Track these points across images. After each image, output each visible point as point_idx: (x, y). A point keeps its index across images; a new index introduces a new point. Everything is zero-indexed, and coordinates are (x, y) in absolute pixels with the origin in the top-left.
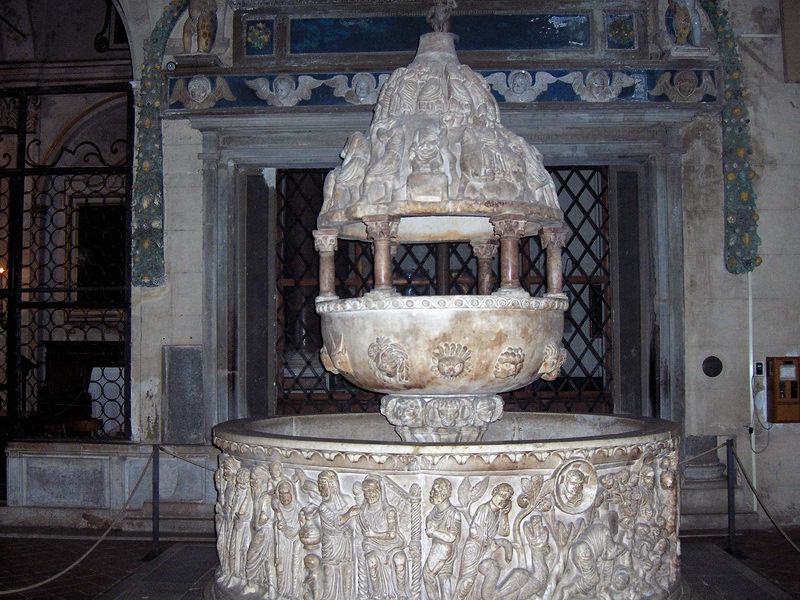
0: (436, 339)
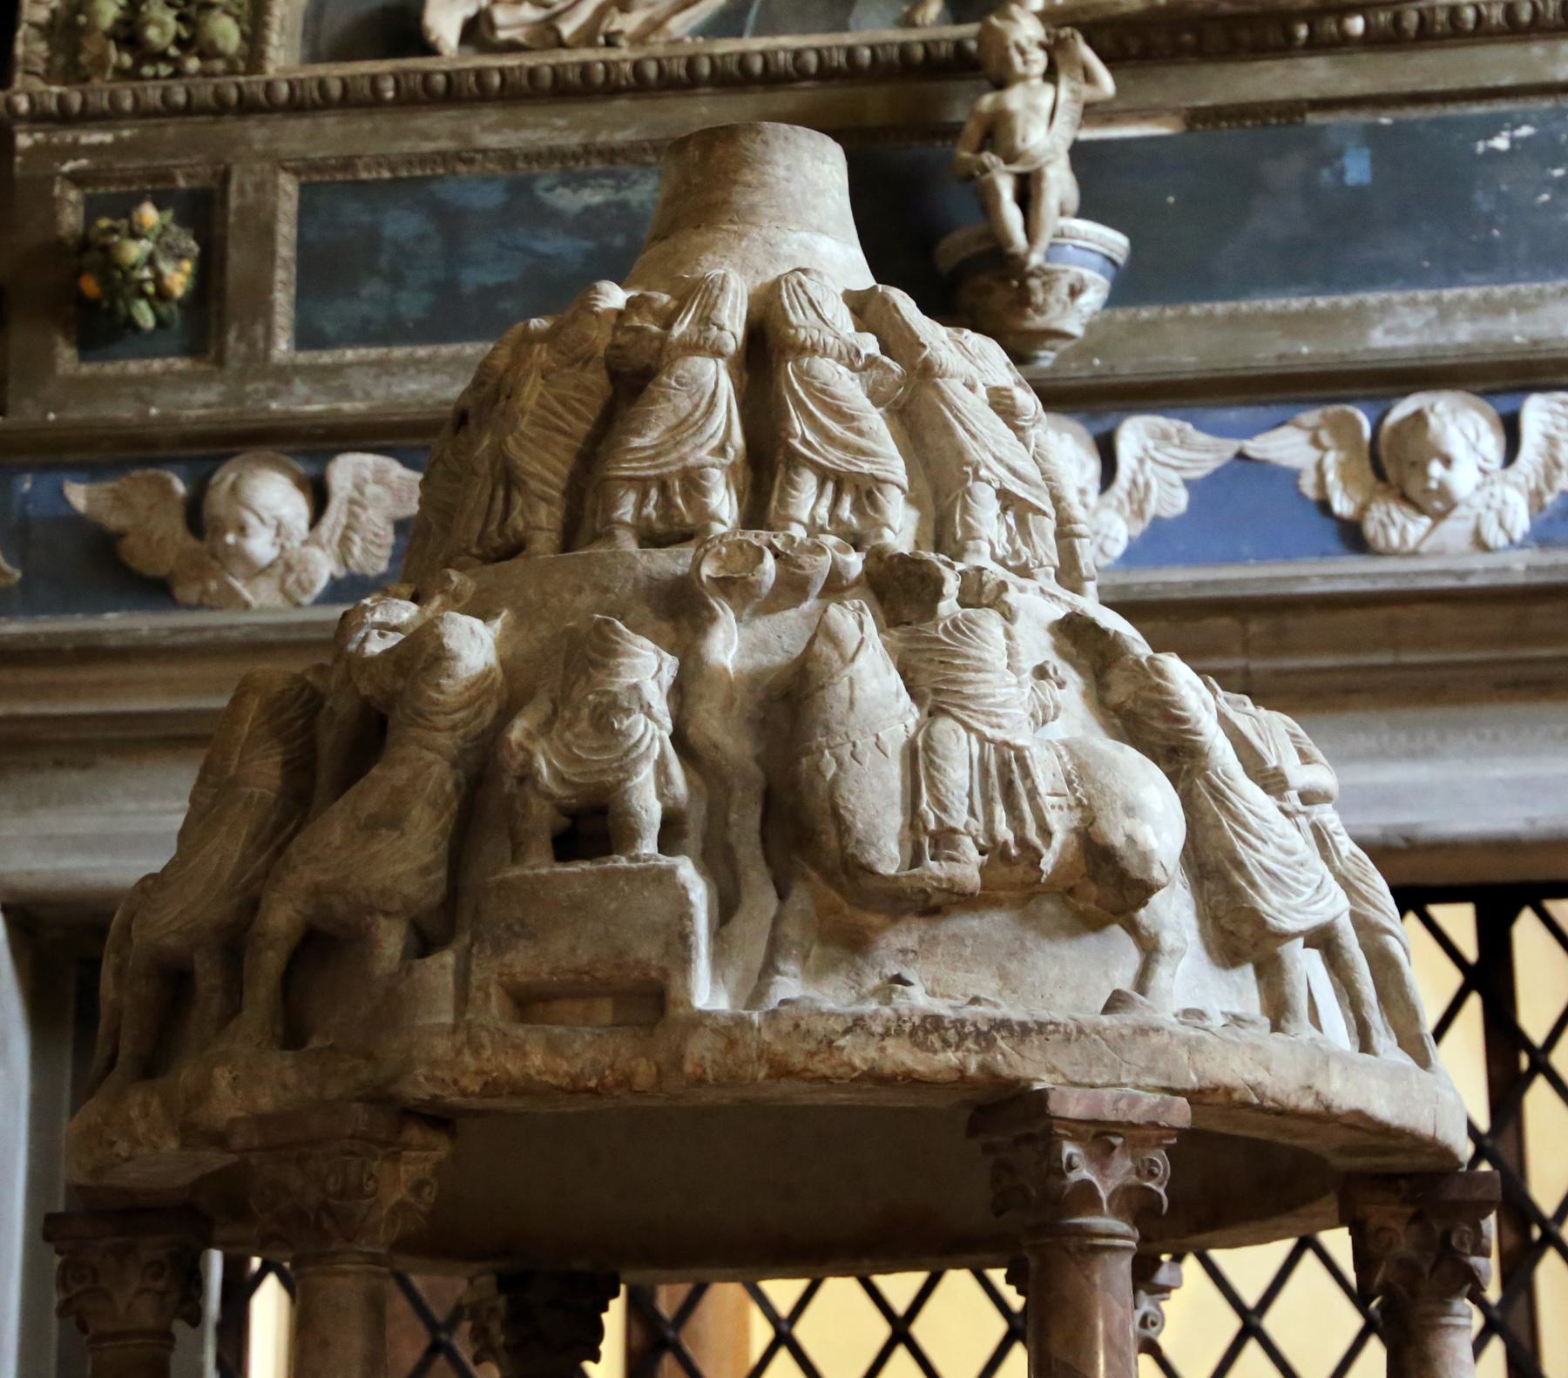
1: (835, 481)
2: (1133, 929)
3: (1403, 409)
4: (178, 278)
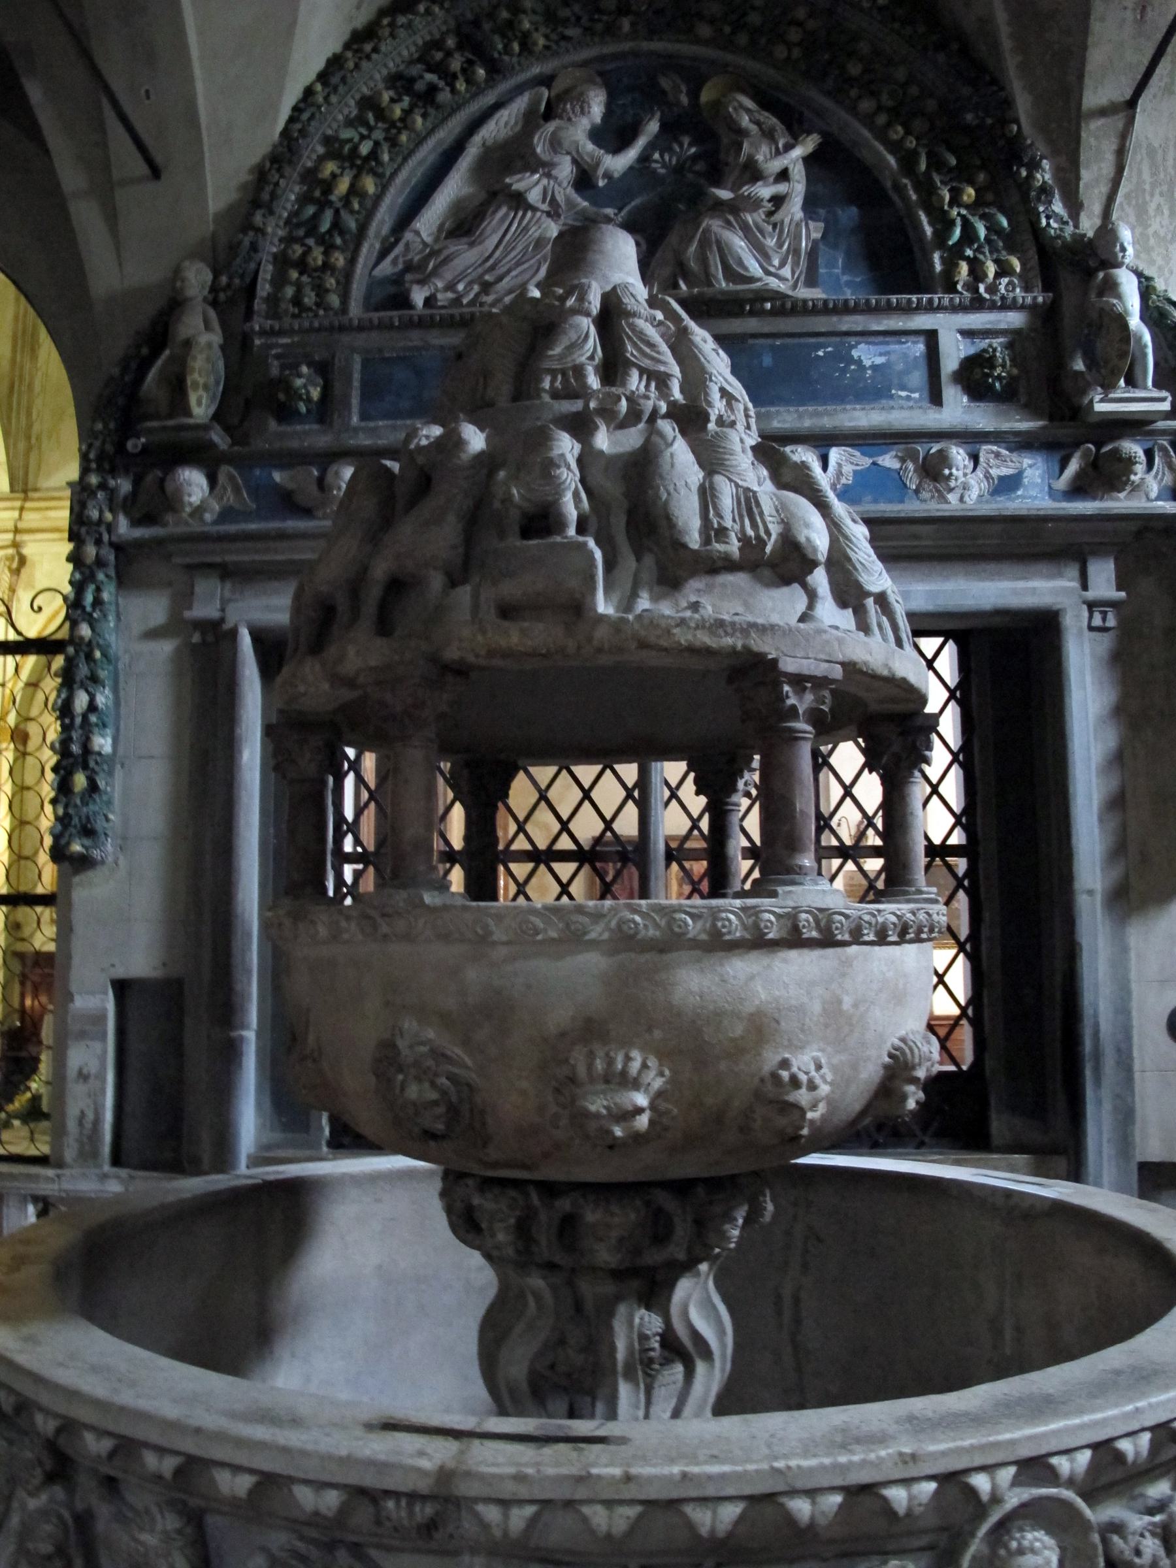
0: (563, 1034)
2: (804, 585)
4: (315, 393)
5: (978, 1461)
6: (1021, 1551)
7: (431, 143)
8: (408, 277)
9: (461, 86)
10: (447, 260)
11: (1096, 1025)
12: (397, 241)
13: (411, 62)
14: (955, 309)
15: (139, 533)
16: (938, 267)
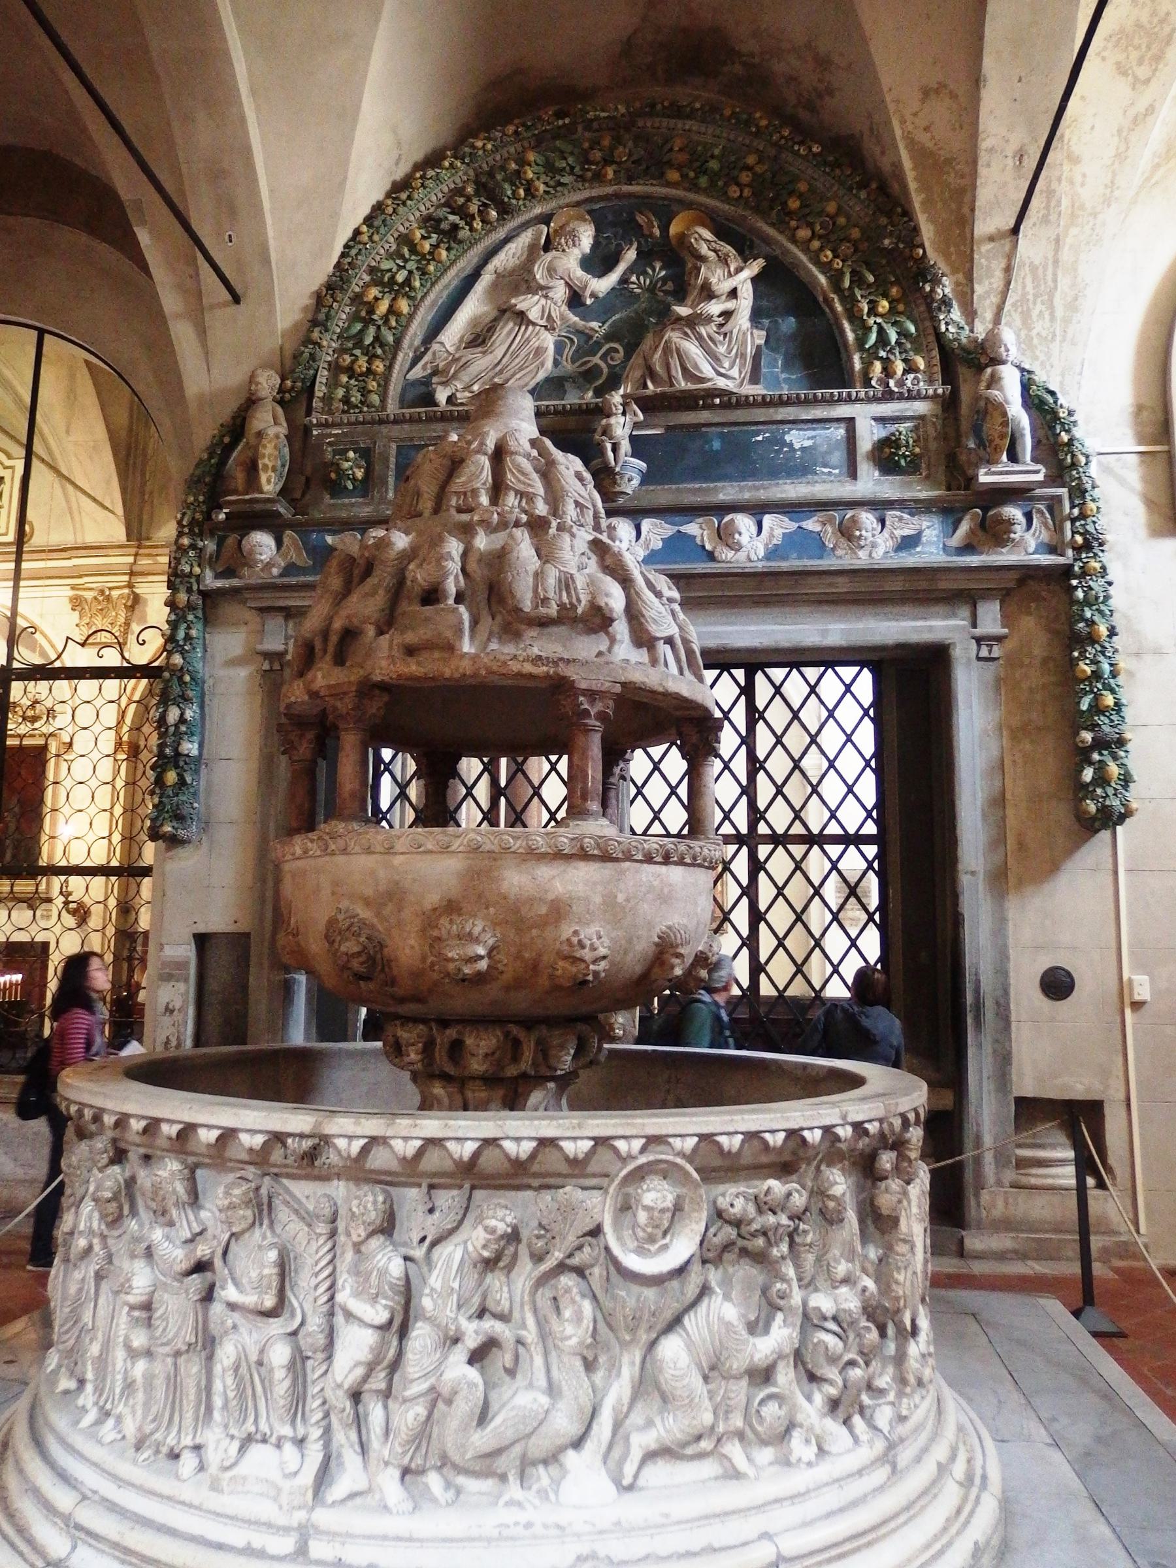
1: (521, 494)
2: (607, 633)
3: (727, 519)
4: (359, 474)
5: (620, 1132)
6: (648, 1190)
7: (452, 272)
8: (435, 380)
9: (477, 224)
10: (465, 365)
11: (978, 982)
12: (427, 350)
13: (438, 207)
14: (870, 400)
15: (219, 584)
16: (858, 366)
